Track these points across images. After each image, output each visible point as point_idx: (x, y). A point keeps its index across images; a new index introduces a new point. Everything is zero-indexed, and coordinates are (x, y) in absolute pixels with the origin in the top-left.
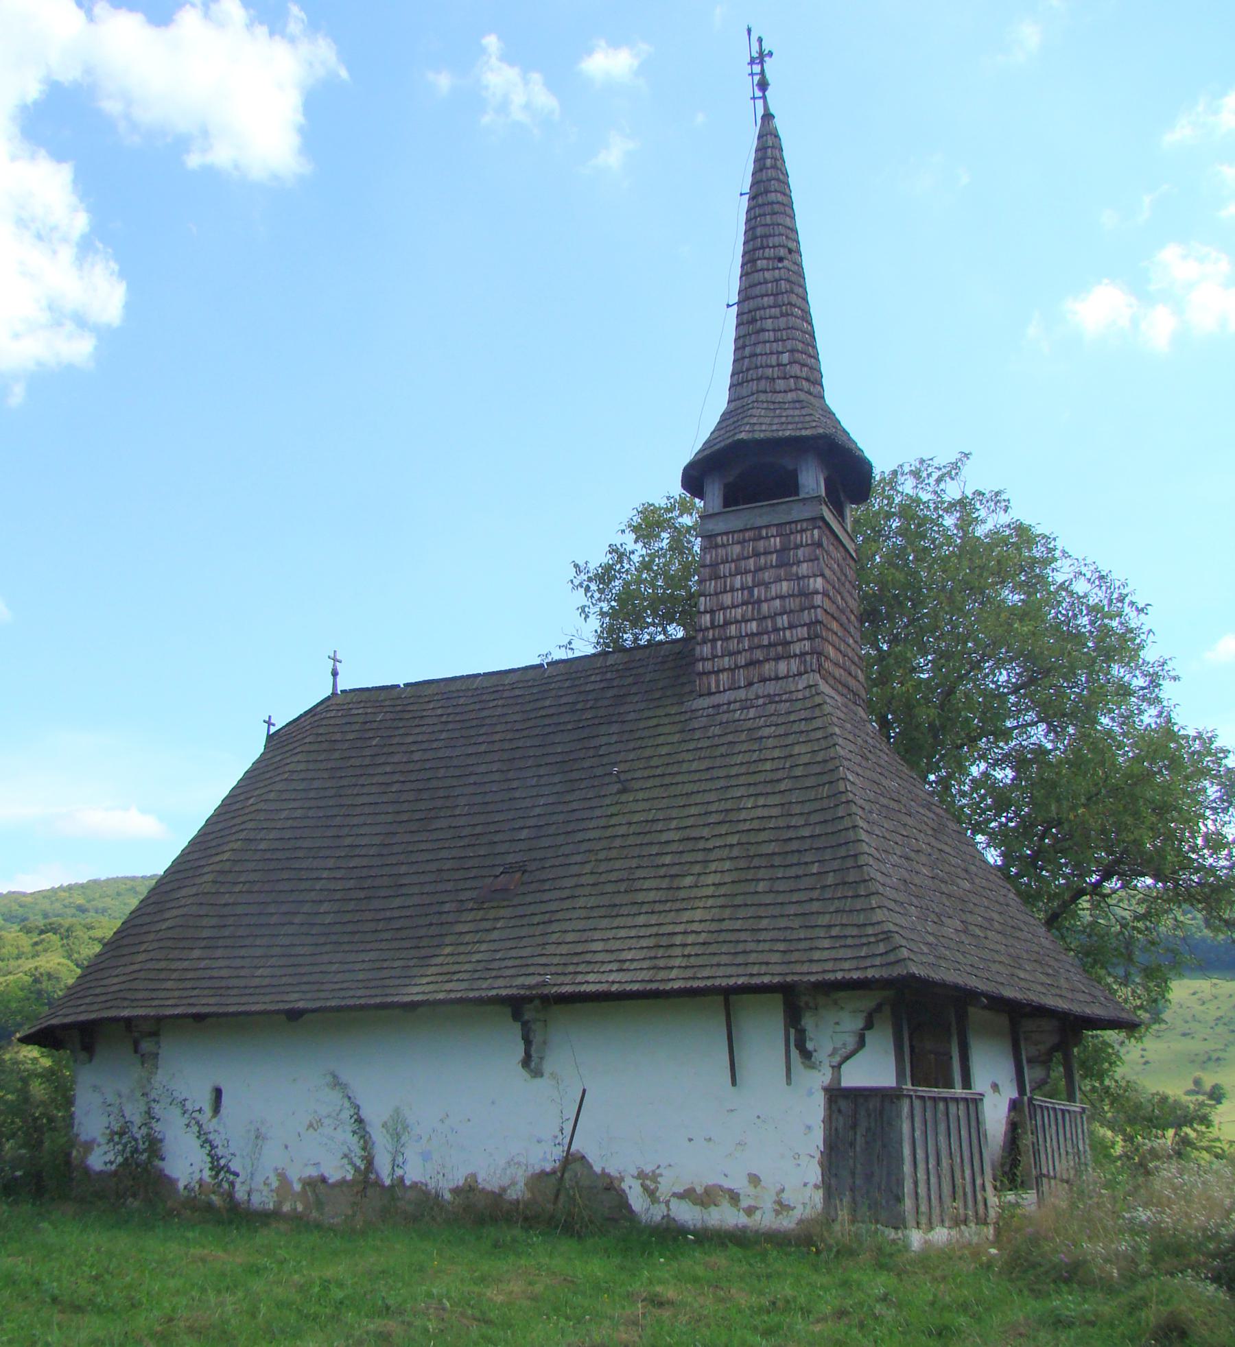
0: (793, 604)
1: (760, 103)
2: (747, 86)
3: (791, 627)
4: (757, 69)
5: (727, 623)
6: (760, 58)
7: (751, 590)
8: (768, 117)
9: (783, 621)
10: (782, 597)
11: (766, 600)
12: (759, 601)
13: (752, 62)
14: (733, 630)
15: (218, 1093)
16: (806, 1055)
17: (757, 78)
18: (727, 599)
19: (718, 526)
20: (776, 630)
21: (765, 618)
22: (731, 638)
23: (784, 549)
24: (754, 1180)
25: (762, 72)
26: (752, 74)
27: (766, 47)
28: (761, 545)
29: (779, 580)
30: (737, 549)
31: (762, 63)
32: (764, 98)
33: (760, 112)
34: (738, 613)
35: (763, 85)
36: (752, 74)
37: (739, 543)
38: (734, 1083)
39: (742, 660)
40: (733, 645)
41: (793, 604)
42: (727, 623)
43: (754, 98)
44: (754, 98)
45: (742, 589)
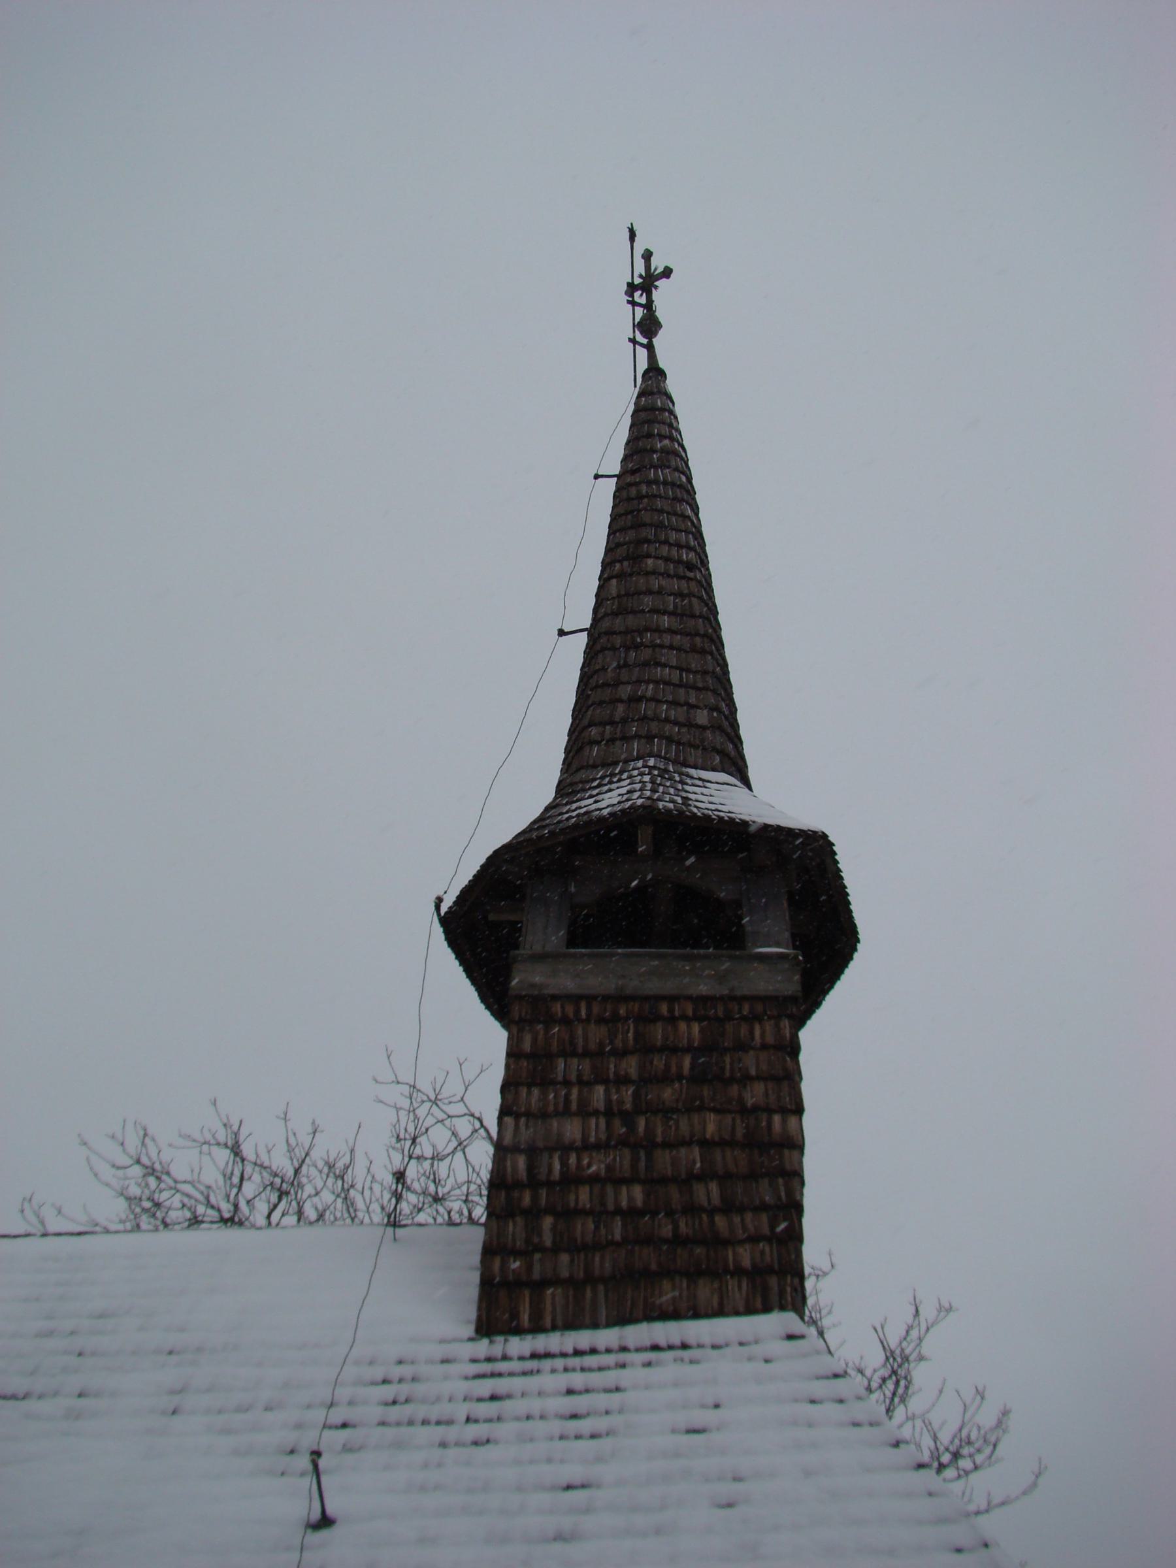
0: (734, 1160)
1: (642, 354)
3: (728, 1207)
5: (571, 1180)
6: (648, 283)
7: (628, 1118)
8: (655, 373)
9: (709, 1193)
10: (705, 1144)
11: (667, 1145)
12: (650, 1145)
13: (631, 288)
14: (584, 1196)
17: (640, 312)
18: (572, 1130)
20: (692, 1209)
21: (664, 1181)
22: (580, 1212)
23: (709, 1047)
25: (649, 306)
28: (658, 1033)
29: (693, 1108)
30: (597, 1033)
32: (650, 348)
33: (643, 365)
34: (596, 1166)
35: (649, 326)
36: (633, 303)
37: (601, 1020)
39: (603, 1264)
40: (584, 1228)
41: (734, 1160)
42: (571, 1180)
44: (633, 341)
45: (609, 1113)
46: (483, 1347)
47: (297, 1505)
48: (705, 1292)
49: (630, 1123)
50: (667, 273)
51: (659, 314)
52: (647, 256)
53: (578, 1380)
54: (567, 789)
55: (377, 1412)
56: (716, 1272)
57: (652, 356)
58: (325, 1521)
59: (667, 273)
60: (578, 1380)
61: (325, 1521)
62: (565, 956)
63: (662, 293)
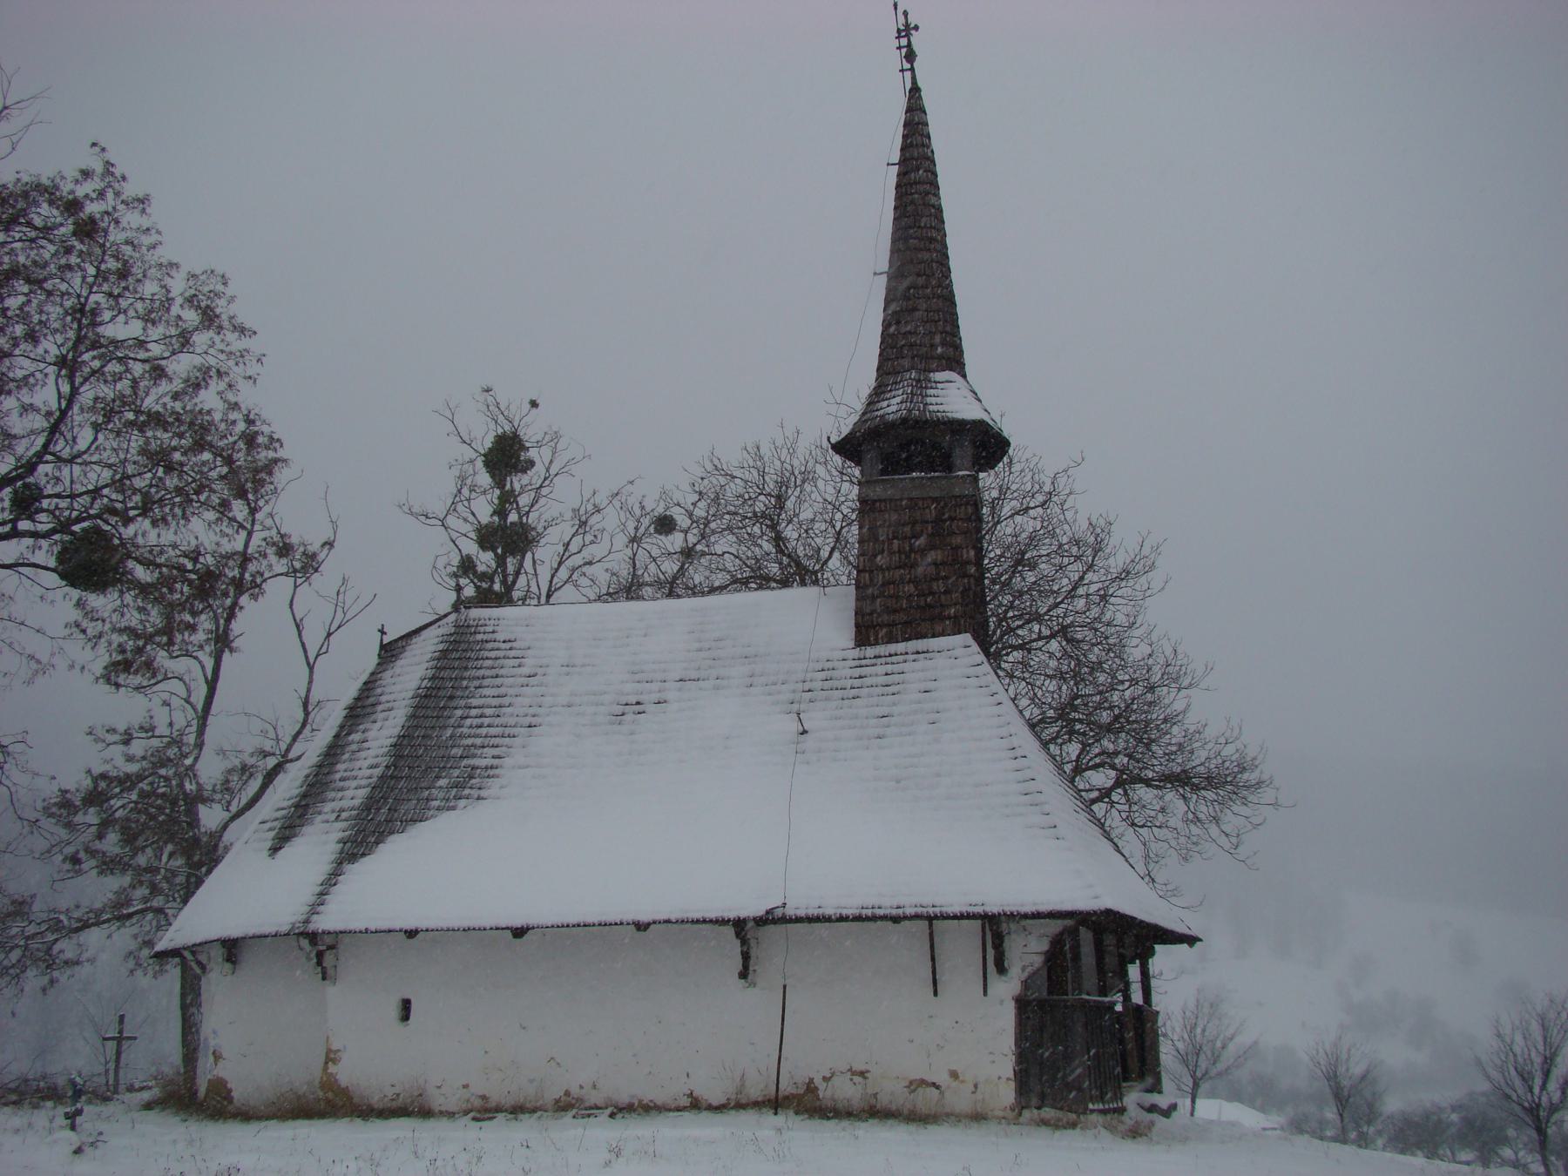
1: (908, 75)
2: (895, 59)
4: (904, 42)
6: (906, 31)
8: (915, 91)
15: (406, 1006)
16: (1001, 969)
17: (904, 51)
19: (877, 492)
23: (938, 521)
24: (954, 1075)
25: (909, 45)
26: (899, 48)
27: (912, 21)
30: (894, 517)
31: (908, 36)
32: (912, 70)
35: (910, 56)
36: (899, 48)
38: (936, 993)
43: (902, 71)
44: (902, 71)
46: (856, 653)
47: (795, 727)
48: (939, 628)
49: (908, 557)
50: (916, 28)
51: (915, 48)
52: (905, 14)
53: (889, 668)
54: (879, 392)
55: (818, 685)
56: (942, 618)
57: (914, 78)
58: (804, 732)
59: (916, 28)
60: (889, 668)
61: (804, 732)
62: (877, 481)
63: (916, 38)
